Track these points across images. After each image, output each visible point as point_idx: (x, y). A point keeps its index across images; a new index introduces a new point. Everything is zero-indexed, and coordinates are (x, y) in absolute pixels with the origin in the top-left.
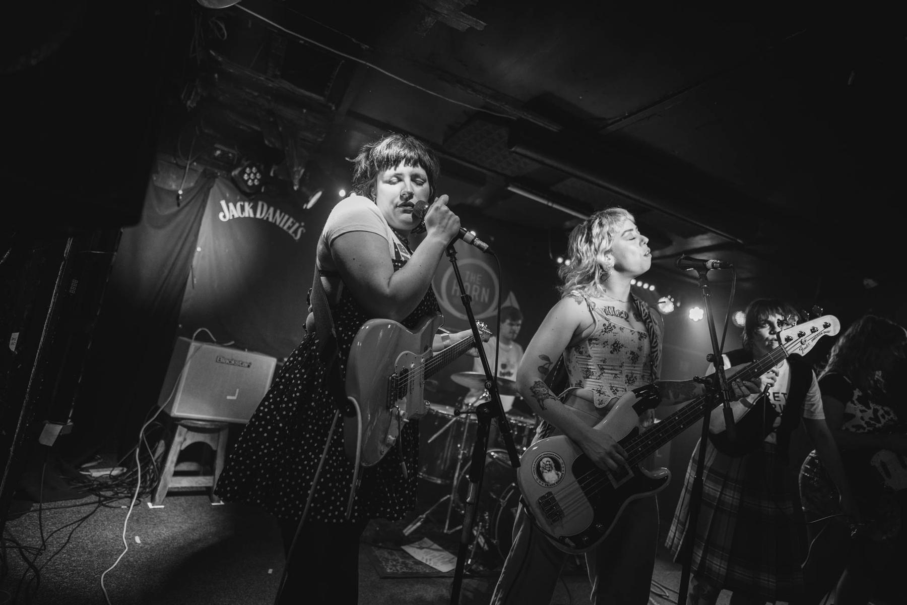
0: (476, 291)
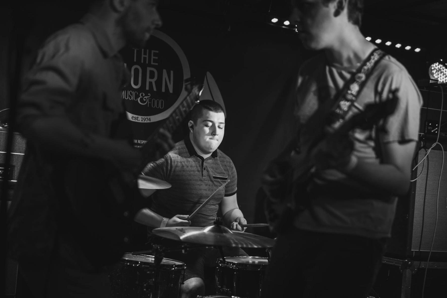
0: (152, 76)
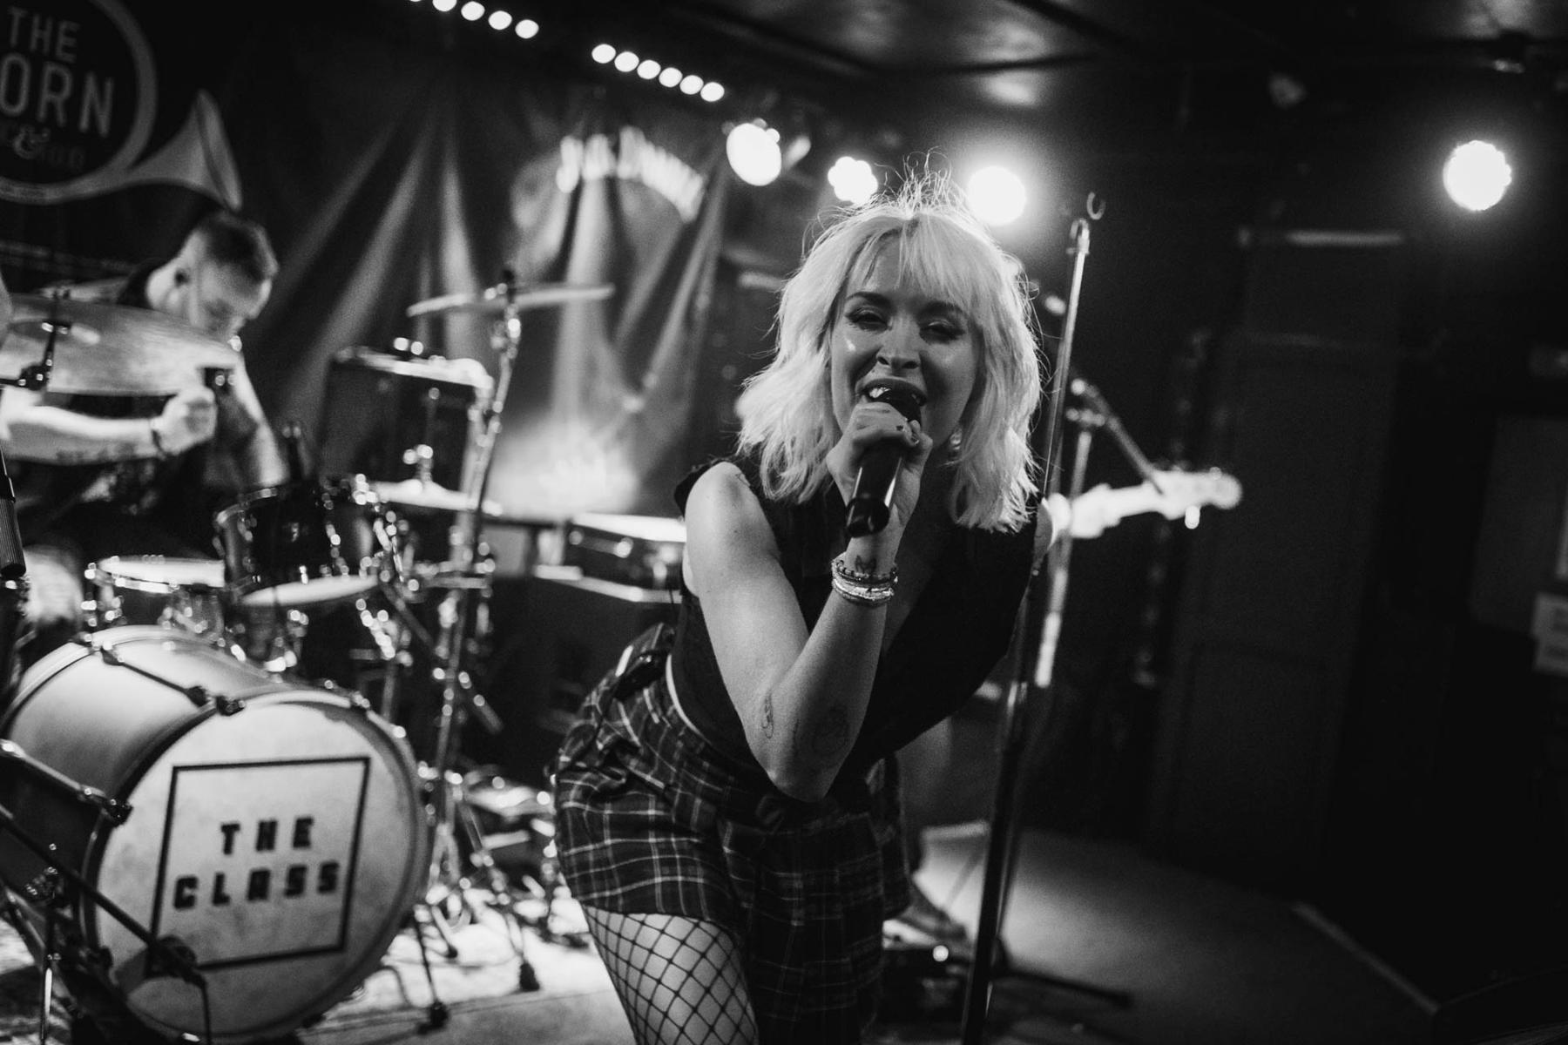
0: (57, 85)
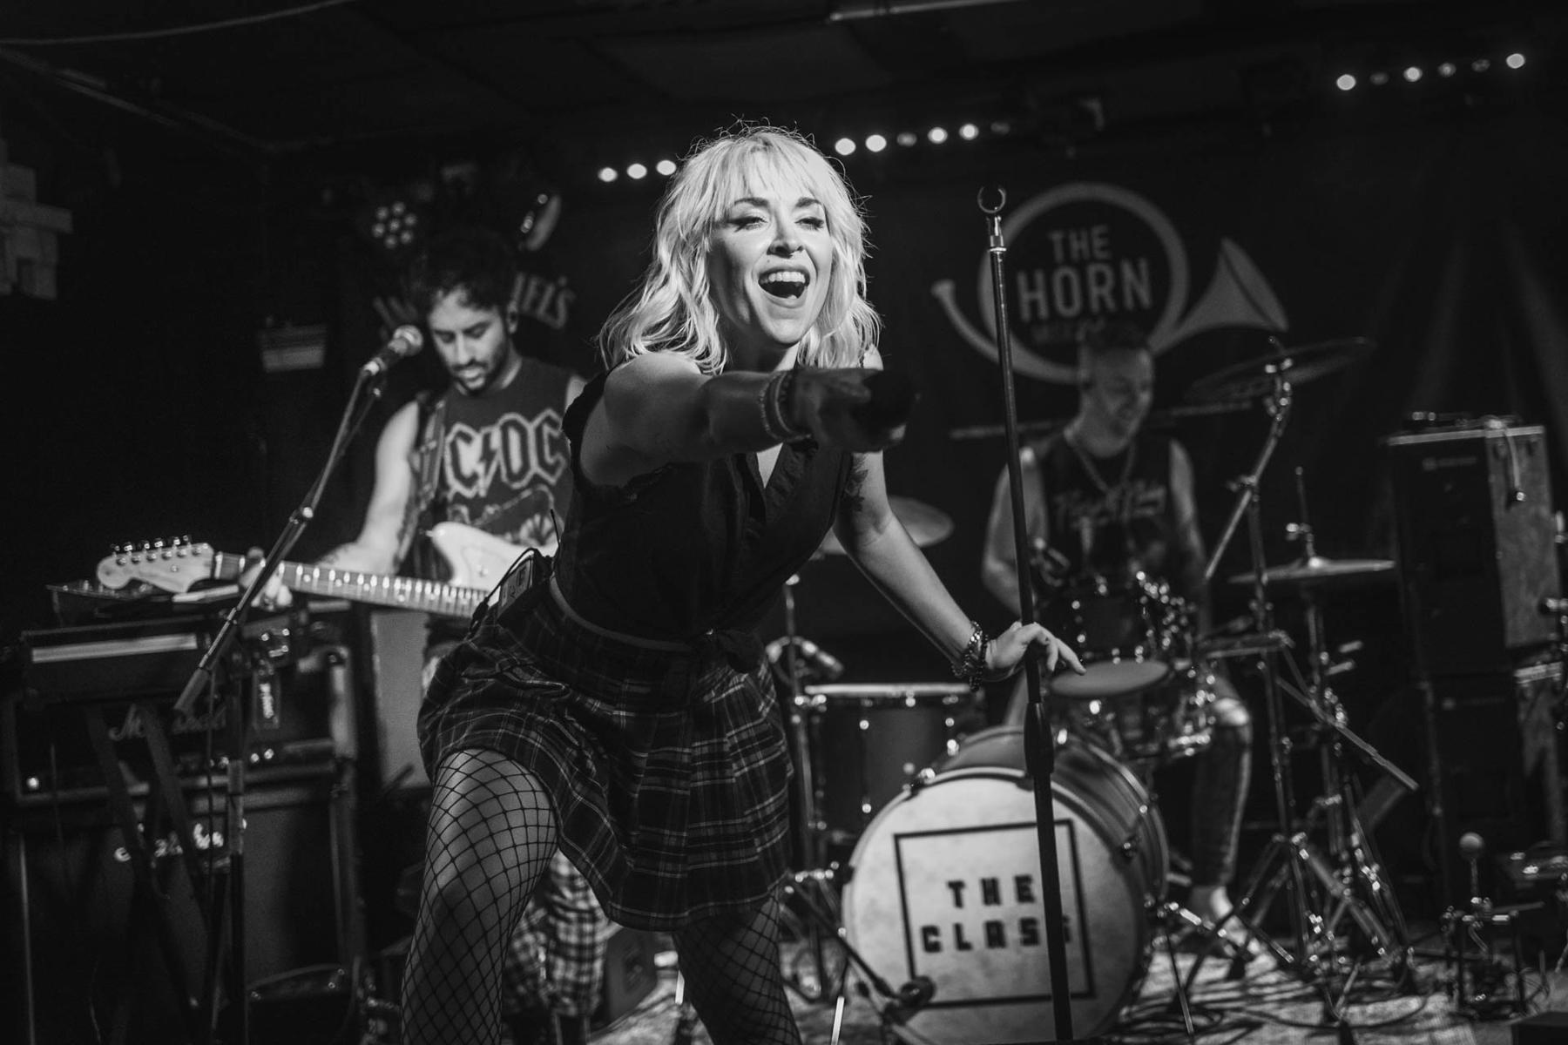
0: (1101, 279)
